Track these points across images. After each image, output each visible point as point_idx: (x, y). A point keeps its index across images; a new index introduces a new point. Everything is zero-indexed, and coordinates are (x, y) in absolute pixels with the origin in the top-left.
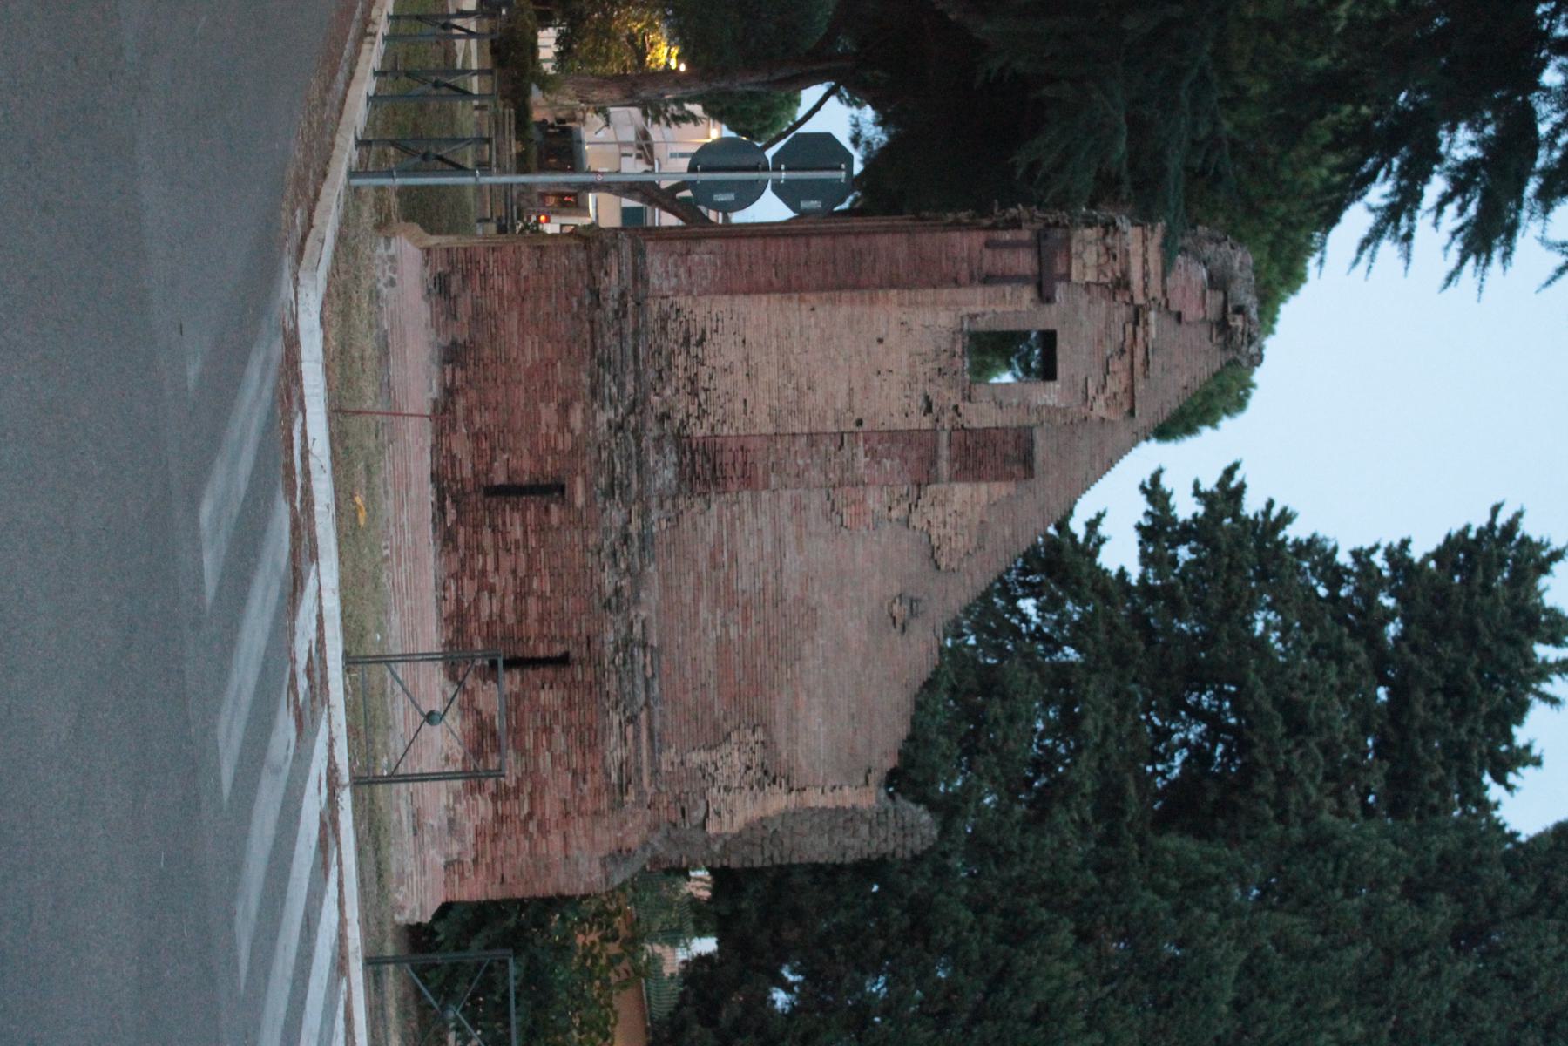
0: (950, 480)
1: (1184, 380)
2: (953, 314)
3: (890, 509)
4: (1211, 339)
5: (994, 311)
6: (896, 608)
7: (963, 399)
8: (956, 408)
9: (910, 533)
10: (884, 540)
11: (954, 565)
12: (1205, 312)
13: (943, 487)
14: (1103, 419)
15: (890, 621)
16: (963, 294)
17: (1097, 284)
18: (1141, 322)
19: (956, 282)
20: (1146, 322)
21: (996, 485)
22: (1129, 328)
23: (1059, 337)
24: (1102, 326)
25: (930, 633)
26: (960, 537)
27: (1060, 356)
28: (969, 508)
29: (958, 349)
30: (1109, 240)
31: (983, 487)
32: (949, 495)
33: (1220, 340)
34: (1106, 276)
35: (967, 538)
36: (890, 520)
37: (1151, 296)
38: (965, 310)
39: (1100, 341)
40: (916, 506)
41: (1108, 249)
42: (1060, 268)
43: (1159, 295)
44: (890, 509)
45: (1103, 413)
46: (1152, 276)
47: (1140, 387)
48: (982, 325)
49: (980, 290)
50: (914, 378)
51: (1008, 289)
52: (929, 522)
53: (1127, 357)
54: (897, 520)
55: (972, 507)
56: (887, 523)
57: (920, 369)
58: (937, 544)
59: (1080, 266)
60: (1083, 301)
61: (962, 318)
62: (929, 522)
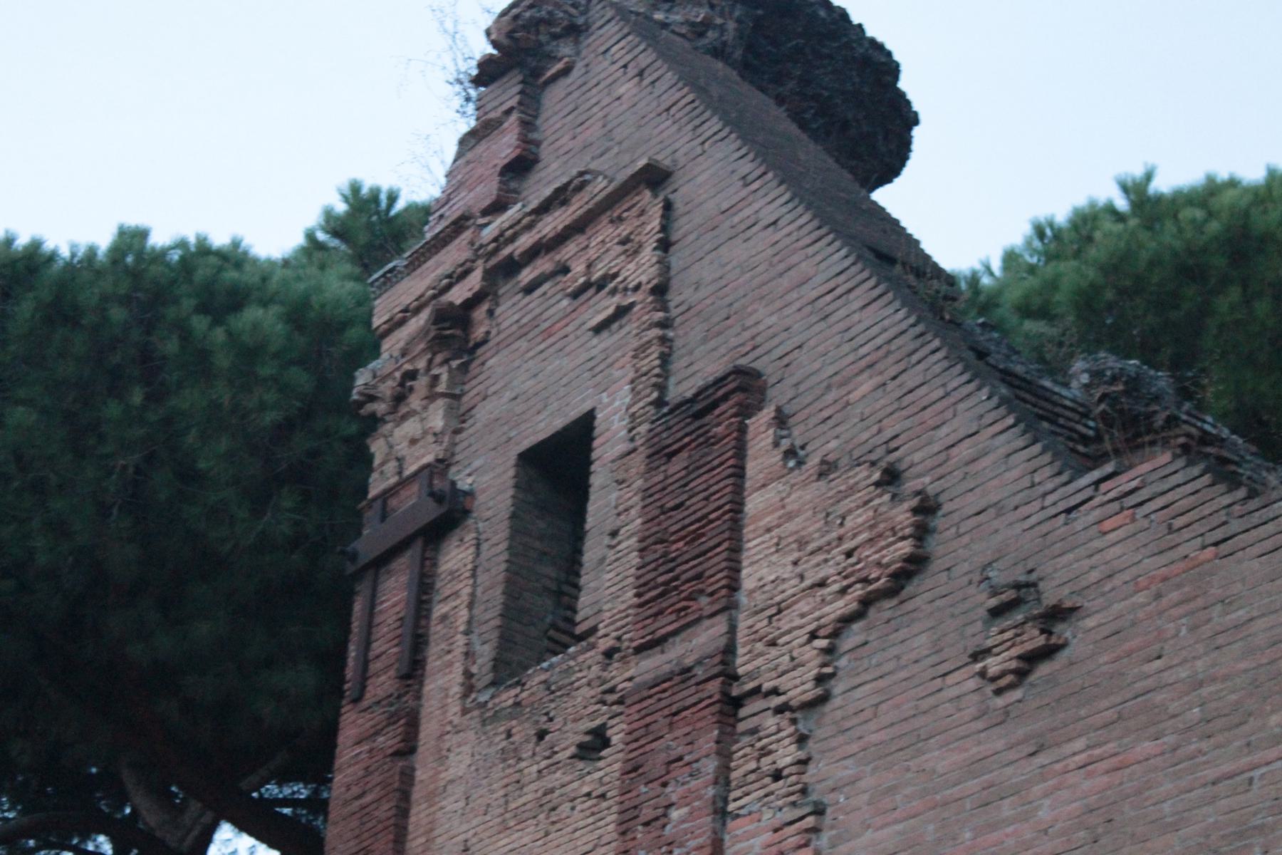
0: (730, 607)
1: (626, 88)
2: (456, 739)
3: (777, 776)
4: (566, 71)
5: (467, 633)
6: (993, 665)
7: (593, 646)
8: (609, 654)
9: (838, 687)
10: (846, 771)
11: (902, 516)
12: (508, 112)
13: (742, 626)
14: (665, 245)
15: (1044, 669)
16: (428, 730)
17: (456, 397)
18: (506, 252)
19: (408, 749)
20: (501, 240)
21: (751, 468)
22: (527, 275)
23: (526, 444)
24: (523, 344)
25: (1084, 518)
26: (849, 523)
27: (559, 423)
28: (790, 527)
29: (507, 697)
30: (380, 408)
31: (754, 503)
32: (760, 597)
33: (565, 49)
34: (436, 378)
35: (847, 504)
36: (804, 762)
37: (467, 254)
38: (455, 708)
39: (548, 333)
40: (775, 692)
41: (399, 399)
42: (410, 498)
43: (467, 235)
44: (777, 776)
45: (648, 254)
46: (440, 271)
47: (599, 188)
48: (485, 652)
49: (431, 686)
50: (547, 805)
51: (439, 610)
52: (813, 636)
53: (570, 249)
54: (802, 740)
55: (790, 517)
56: (812, 769)
57: (529, 795)
58: (858, 591)
59: (418, 450)
60: (483, 414)
61: (465, 711)
62: (813, 636)
